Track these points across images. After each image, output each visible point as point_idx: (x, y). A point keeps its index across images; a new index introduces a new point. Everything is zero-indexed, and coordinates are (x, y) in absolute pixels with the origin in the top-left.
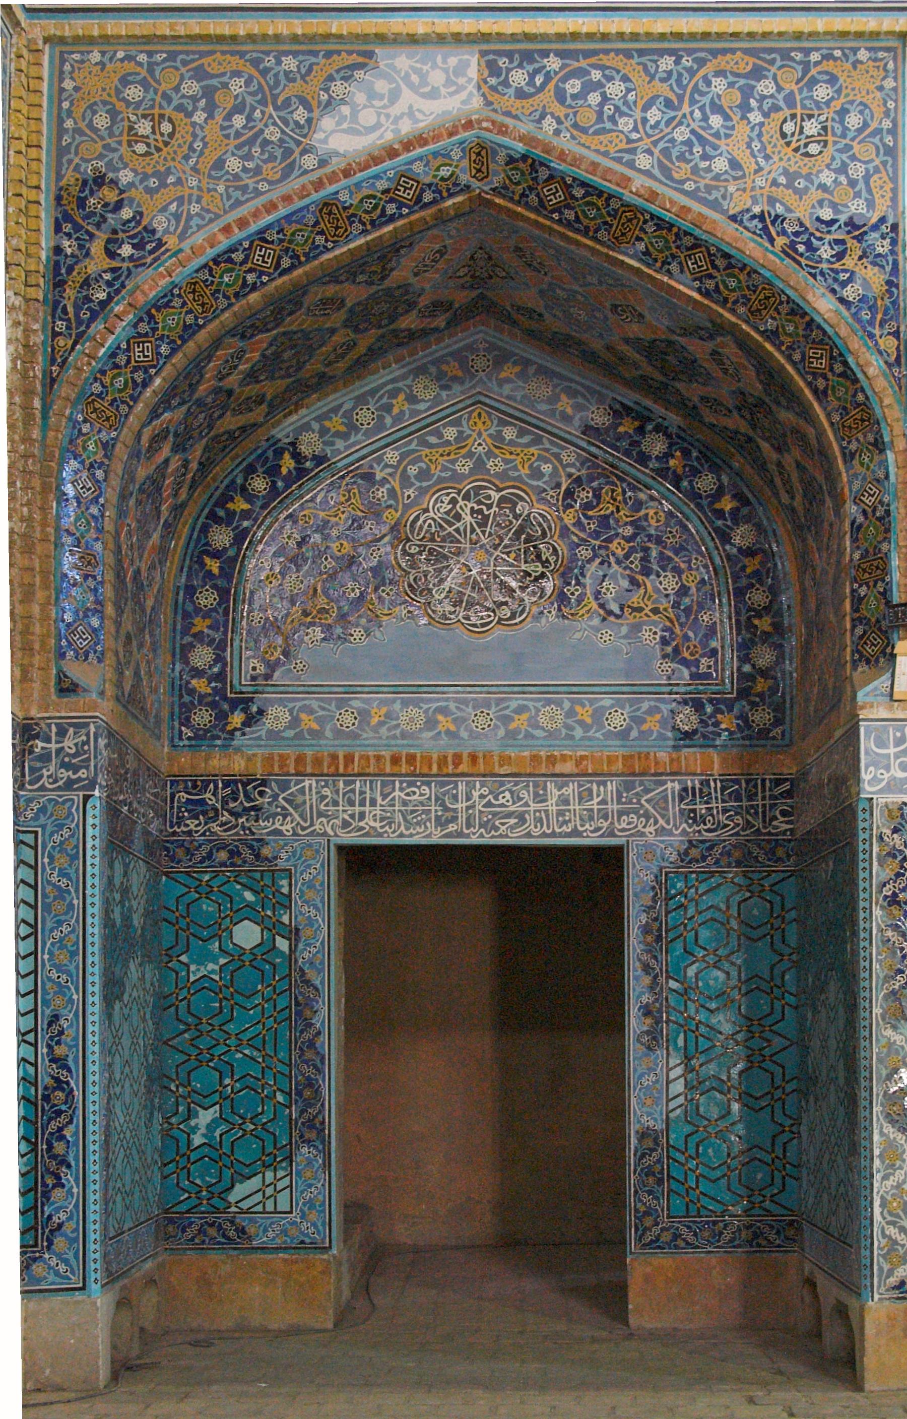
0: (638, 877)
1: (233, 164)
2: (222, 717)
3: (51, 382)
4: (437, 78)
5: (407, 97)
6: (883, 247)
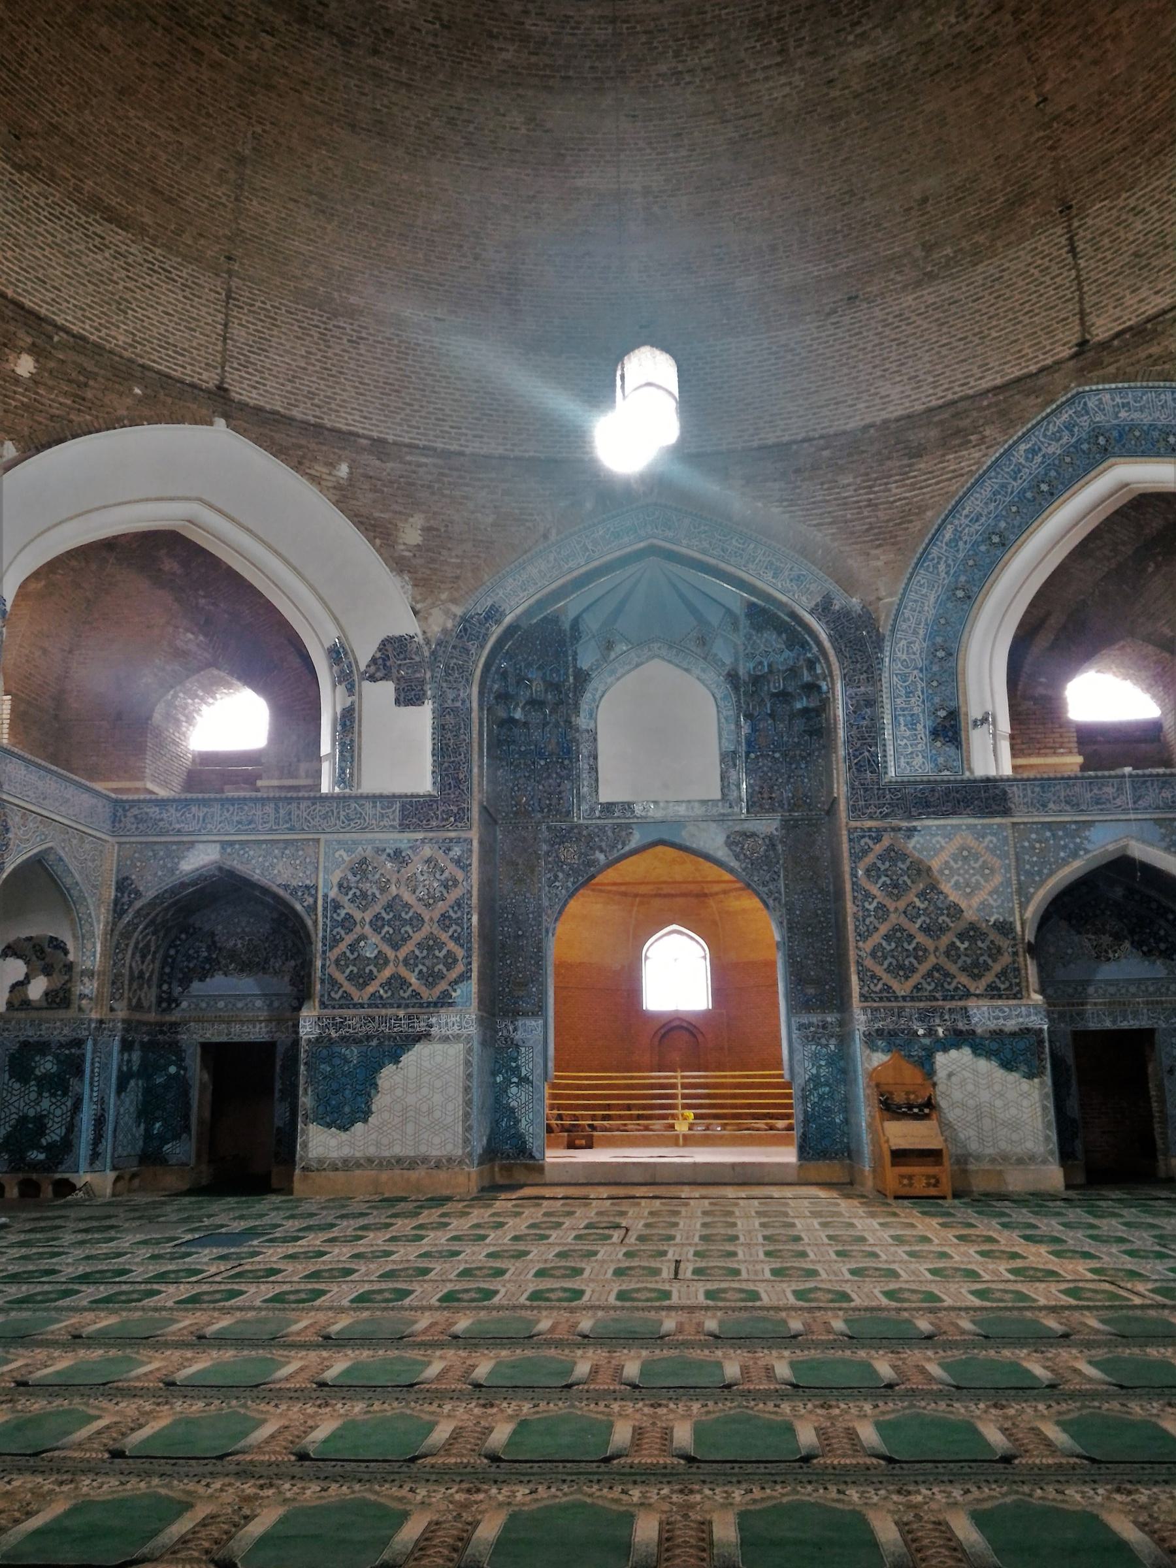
0: (280, 1050)
1: (160, 873)
2: (169, 1005)
3: (112, 930)
4: (209, 851)
5: (202, 856)
6: (313, 892)
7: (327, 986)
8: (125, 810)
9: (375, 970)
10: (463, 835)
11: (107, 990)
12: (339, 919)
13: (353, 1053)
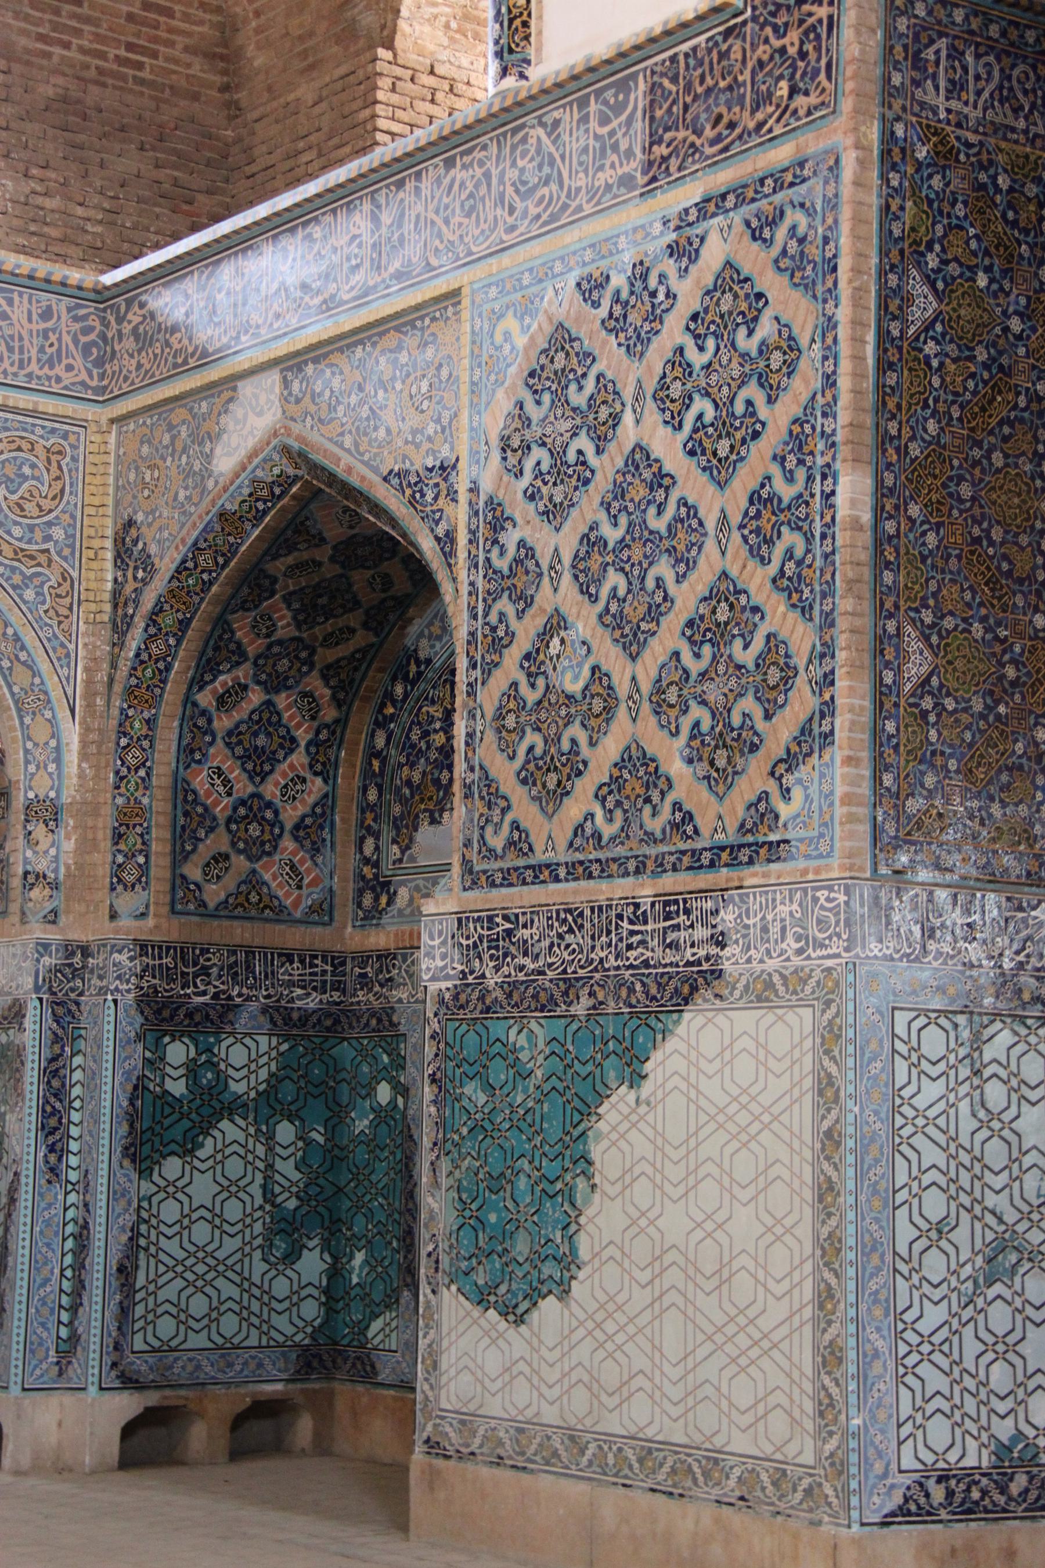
7: (479, 806)
8: (120, 320)
9: (582, 737)
10: (812, 143)
11: (102, 860)
12: (502, 564)
13: (530, 1038)
